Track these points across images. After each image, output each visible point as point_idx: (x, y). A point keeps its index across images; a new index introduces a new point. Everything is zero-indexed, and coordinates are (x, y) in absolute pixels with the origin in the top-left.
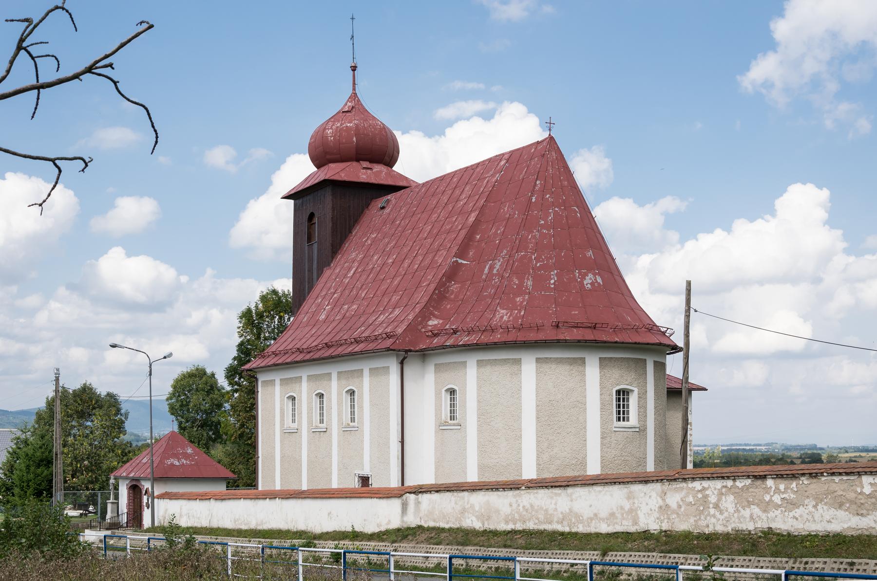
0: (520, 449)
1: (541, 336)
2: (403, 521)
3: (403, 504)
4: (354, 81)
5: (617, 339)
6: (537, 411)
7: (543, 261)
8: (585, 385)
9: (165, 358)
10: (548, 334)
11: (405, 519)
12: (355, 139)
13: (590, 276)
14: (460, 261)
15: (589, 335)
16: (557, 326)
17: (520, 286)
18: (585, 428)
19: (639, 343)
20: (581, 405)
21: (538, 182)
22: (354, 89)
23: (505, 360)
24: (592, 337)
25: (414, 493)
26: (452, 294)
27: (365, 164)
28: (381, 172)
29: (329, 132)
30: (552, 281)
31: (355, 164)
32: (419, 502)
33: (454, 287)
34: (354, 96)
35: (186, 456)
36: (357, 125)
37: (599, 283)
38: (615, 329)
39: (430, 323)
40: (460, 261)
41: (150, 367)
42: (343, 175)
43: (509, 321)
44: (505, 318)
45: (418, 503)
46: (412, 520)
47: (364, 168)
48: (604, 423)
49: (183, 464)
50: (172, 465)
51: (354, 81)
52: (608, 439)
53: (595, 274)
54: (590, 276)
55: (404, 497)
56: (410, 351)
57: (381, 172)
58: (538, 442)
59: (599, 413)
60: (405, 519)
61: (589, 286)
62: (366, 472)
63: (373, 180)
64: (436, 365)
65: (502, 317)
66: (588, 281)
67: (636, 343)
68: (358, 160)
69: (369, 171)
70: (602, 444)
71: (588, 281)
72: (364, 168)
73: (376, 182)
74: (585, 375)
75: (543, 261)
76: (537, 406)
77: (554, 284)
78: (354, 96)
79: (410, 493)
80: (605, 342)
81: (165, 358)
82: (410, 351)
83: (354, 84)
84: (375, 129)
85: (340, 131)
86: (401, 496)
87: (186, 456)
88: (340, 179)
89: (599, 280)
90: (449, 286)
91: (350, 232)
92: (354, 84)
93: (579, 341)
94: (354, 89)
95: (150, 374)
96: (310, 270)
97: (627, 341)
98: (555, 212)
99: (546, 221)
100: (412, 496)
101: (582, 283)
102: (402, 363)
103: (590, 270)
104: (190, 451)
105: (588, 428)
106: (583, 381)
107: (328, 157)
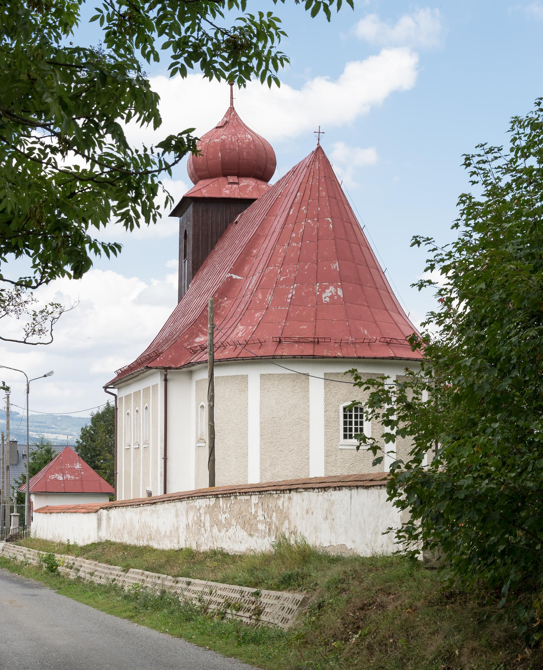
0: (247, 466)
2: (98, 536)
3: (98, 519)
4: (232, 95)
5: (339, 354)
6: (261, 428)
9: (45, 376)
10: (269, 350)
11: (100, 534)
12: (220, 155)
13: (332, 288)
14: (234, 277)
15: (308, 350)
16: (280, 342)
17: (262, 301)
18: (308, 446)
19: (364, 358)
20: (304, 422)
22: (232, 103)
23: (235, 377)
24: (311, 353)
25: (106, 508)
26: (222, 311)
27: (231, 179)
28: (247, 186)
30: (290, 296)
31: (221, 179)
33: (226, 303)
34: (232, 109)
35: (72, 471)
38: (341, 344)
39: (198, 340)
40: (234, 277)
41: (28, 385)
42: (204, 191)
44: (240, 335)
45: (109, 518)
46: (105, 535)
47: (230, 183)
48: (329, 440)
49: (67, 479)
50: (56, 480)
51: (232, 95)
52: (333, 457)
53: (336, 287)
54: (332, 288)
56: (170, 368)
57: (247, 186)
58: (262, 459)
59: (323, 430)
60: (100, 534)
61: (327, 299)
62: (150, 489)
63: (237, 196)
65: (237, 334)
66: (327, 294)
68: (225, 175)
69: (235, 186)
70: (326, 462)
71: (326, 296)
72: (230, 183)
73: (239, 197)
74: (308, 391)
76: (261, 423)
77: (291, 298)
78: (232, 109)
79: (103, 508)
80: (323, 357)
81: (45, 376)
82: (170, 368)
83: (232, 98)
84: (244, 143)
86: (96, 511)
87: (72, 471)
89: (340, 292)
90: (221, 303)
91: (213, 248)
92: (232, 98)
93: (294, 357)
94: (232, 103)
95: (28, 392)
96: (184, 288)
97: (351, 356)
98: (307, 225)
99: (297, 234)
100: (104, 512)
101: (320, 296)
102: (166, 380)
103: (331, 283)
104: (78, 466)
105: (311, 446)
106: (306, 398)
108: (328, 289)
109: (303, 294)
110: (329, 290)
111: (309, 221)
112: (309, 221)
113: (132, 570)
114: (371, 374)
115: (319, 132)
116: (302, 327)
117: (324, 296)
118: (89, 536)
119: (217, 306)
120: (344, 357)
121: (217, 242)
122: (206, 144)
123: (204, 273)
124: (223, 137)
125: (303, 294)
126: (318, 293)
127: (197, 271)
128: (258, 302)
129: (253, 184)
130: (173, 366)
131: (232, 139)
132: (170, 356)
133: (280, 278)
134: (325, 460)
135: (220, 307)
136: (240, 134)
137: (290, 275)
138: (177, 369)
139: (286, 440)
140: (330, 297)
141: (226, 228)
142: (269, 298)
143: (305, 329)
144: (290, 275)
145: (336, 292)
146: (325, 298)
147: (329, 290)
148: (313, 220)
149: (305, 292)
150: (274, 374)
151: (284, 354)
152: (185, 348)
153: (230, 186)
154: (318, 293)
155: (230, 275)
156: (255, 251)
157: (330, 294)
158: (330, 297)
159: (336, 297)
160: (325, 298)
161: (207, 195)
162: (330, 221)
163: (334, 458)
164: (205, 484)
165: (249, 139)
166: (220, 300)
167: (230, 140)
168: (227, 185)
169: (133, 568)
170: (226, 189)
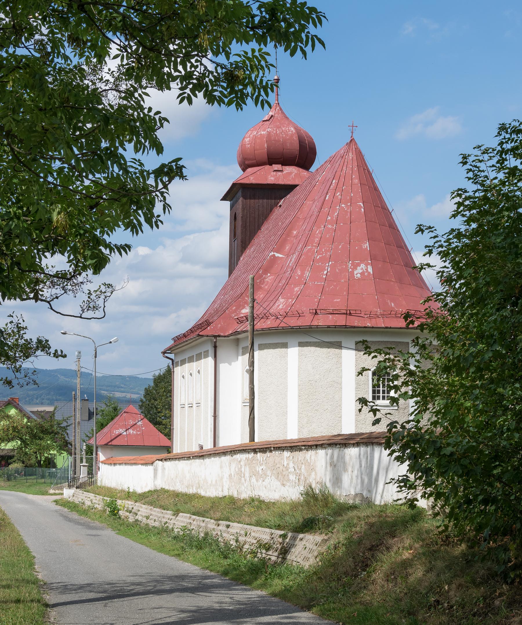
0: (286, 424)
1: (299, 322)
5: (369, 325)
6: (299, 390)
7: (322, 254)
8: (341, 366)
10: (306, 321)
11: (156, 483)
12: (266, 145)
14: (277, 255)
15: (341, 320)
16: (316, 313)
17: (301, 276)
18: (340, 406)
19: (391, 328)
21: (334, 181)
26: (266, 285)
29: (247, 140)
30: (325, 272)
31: (267, 167)
32: (164, 468)
36: (269, 133)
37: (369, 273)
40: (277, 255)
43: (282, 309)
44: (280, 307)
45: (164, 469)
46: (160, 484)
53: (366, 265)
54: (363, 266)
55: (155, 464)
56: (219, 336)
57: (290, 173)
58: (299, 418)
61: (359, 275)
63: (281, 182)
64: (243, 348)
65: (279, 305)
66: (359, 270)
67: (386, 328)
68: (271, 164)
69: (280, 173)
71: (358, 273)
73: (283, 183)
74: (341, 357)
75: (322, 254)
79: (158, 460)
82: (219, 336)
84: (287, 135)
85: (255, 137)
88: (248, 182)
89: (370, 269)
90: (265, 278)
91: (259, 228)
95: (96, 357)
102: (215, 347)
103: (362, 261)
105: (343, 406)
107: (247, 162)
108: (359, 266)
109: (337, 270)
110: (360, 268)
111: (343, 206)
112: (343, 206)
113: (181, 514)
114: (397, 342)
115: (353, 126)
116: (336, 300)
117: (355, 272)
118: (147, 484)
119: (261, 281)
120: (373, 327)
121: (263, 223)
122: (254, 135)
123: (250, 251)
124: (269, 130)
125: (337, 270)
126: (350, 270)
127: (245, 249)
128: (297, 278)
129: (296, 172)
130: (222, 334)
131: (277, 132)
132: (219, 326)
133: (317, 256)
134: (356, 418)
135: (264, 282)
136: (284, 127)
137: (326, 253)
138: (225, 337)
139: (321, 400)
140: (361, 274)
141: (271, 211)
142: (307, 274)
143: (338, 303)
144: (326, 253)
145: (367, 269)
146: (356, 274)
147: (360, 268)
148: (347, 205)
149: (339, 269)
150: (310, 342)
151: (320, 324)
152: (233, 318)
153: (275, 173)
154: (350, 270)
155: (272, 253)
156: (295, 232)
157: (361, 271)
158: (361, 274)
159: (366, 274)
160: (356, 274)
161: (254, 182)
162: (362, 205)
163: (363, 417)
164: (247, 440)
165: (292, 132)
166: (264, 276)
167: (275, 132)
168: (272, 173)
169: (182, 512)
170: (272, 176)
